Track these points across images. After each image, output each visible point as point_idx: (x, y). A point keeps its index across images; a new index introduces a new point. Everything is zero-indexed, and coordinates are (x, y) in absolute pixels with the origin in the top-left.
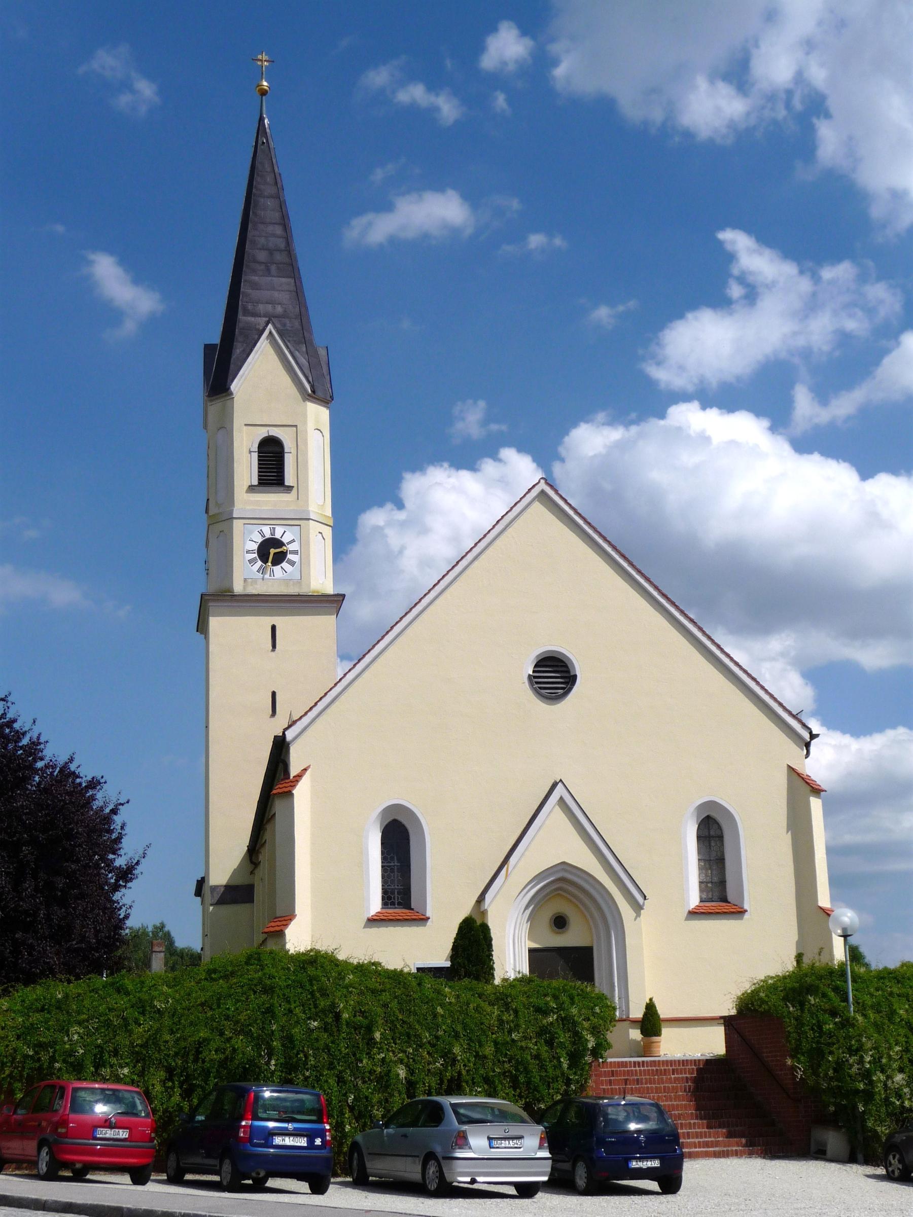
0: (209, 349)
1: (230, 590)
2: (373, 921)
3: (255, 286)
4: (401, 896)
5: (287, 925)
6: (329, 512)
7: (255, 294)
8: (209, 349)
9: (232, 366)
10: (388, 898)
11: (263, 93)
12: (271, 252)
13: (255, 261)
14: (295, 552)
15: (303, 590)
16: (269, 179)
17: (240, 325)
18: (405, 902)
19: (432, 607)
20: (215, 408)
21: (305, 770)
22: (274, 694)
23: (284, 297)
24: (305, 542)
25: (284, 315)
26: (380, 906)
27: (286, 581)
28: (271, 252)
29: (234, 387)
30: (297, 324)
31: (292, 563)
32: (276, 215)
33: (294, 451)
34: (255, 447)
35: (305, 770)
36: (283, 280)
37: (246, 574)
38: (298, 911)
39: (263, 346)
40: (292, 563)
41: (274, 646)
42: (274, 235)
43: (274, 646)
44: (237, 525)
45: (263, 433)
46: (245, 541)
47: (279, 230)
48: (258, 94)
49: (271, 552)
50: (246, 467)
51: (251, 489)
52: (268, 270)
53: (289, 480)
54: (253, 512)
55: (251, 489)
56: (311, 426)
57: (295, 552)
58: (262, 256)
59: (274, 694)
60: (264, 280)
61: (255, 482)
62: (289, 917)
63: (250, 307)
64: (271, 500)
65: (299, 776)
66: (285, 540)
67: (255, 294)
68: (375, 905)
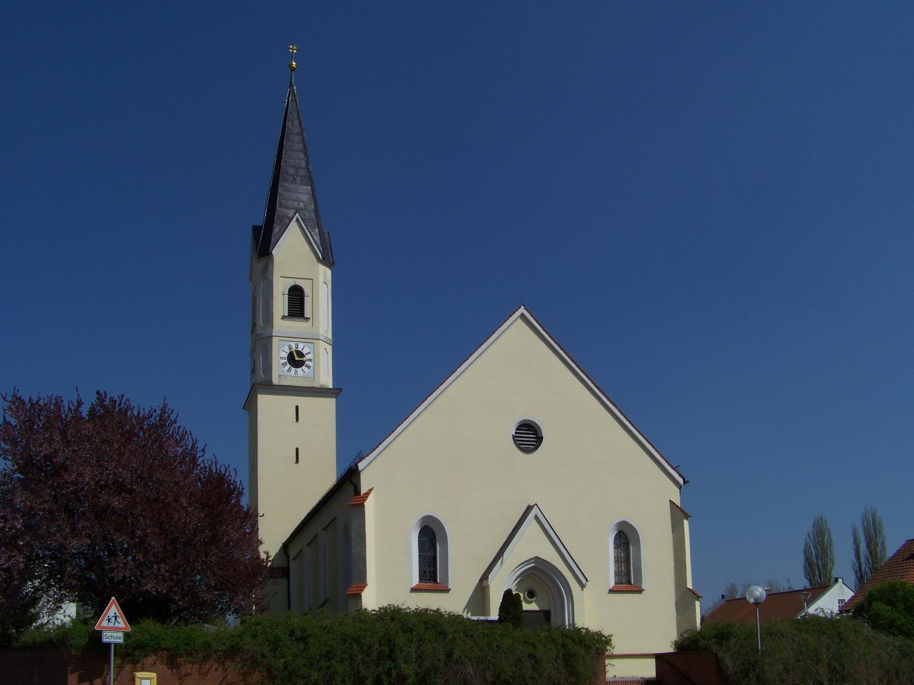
0: (256, 229)
1: (271, 382)
2: (414, 590)
3: (288, 190)
4: (431, 573)
5: (362, 590)
6: (330, 337)
7: (286, 194)
8: (256, 229)
9: (273, 239)
10: (422, 578)
11: (293, 69)
12: (297, 169)
13: (287, 174)
14: (310, 360)
15: (316, 385)
16: (296, 122)
17: (277, 213)
18: (433, 578)
19: (451, 386)
20: (259, 266)
21: (371, 490)
22: (297, 450)
23: (305, 198)
24: (315, 352)
25: (305, 209)
26: (417, 580)
27: (306, 378)
28: (297, 169)
29: (274, 252)
30: (313, 215)
31: (309, 367)
32: (301, 146)
33: (310, 295)
34: (287, 292)
35: (371, 490)
36: (305, 187)
37: (281, 373)
38: (368, 581)
39: (293, 227)
40: (309, 367)
41: (297, 419)
42: (300, 159)
43: (297, 419)
44: (275, 341)
45: (291, 283)
46: (279, 353)
47: (302, 155)
48: (289, 70)
49: (295, 360)
50: (280, 304)
51: (283, 317)
52: (295, 179)
53: (307, 313)
54: (285, 332)
55: (283, 317)
56: (321, 280)
57: (310, 360)
58: (291, 171)
59: (297, 450)
60: (292, 187)
61: (286, 314)
62: (362, 583)
63: (284, 202)
64: (295, 325)
65: (367, 494)
66: (304, 352)
67: (286, 194)
68: (415, 581)
